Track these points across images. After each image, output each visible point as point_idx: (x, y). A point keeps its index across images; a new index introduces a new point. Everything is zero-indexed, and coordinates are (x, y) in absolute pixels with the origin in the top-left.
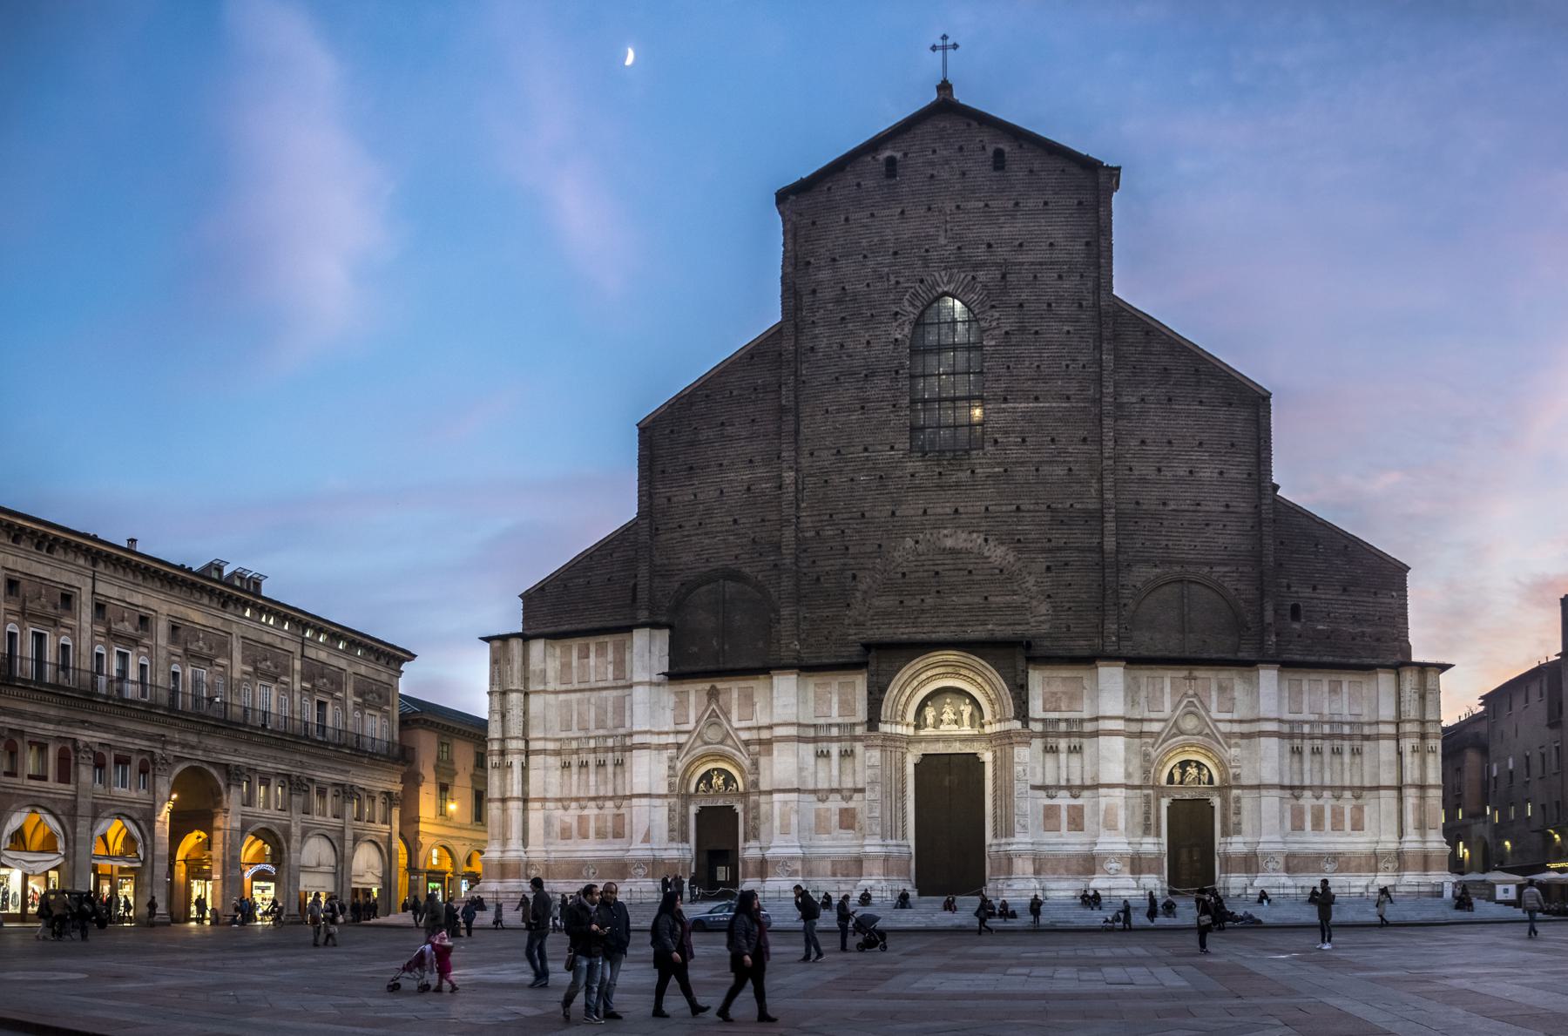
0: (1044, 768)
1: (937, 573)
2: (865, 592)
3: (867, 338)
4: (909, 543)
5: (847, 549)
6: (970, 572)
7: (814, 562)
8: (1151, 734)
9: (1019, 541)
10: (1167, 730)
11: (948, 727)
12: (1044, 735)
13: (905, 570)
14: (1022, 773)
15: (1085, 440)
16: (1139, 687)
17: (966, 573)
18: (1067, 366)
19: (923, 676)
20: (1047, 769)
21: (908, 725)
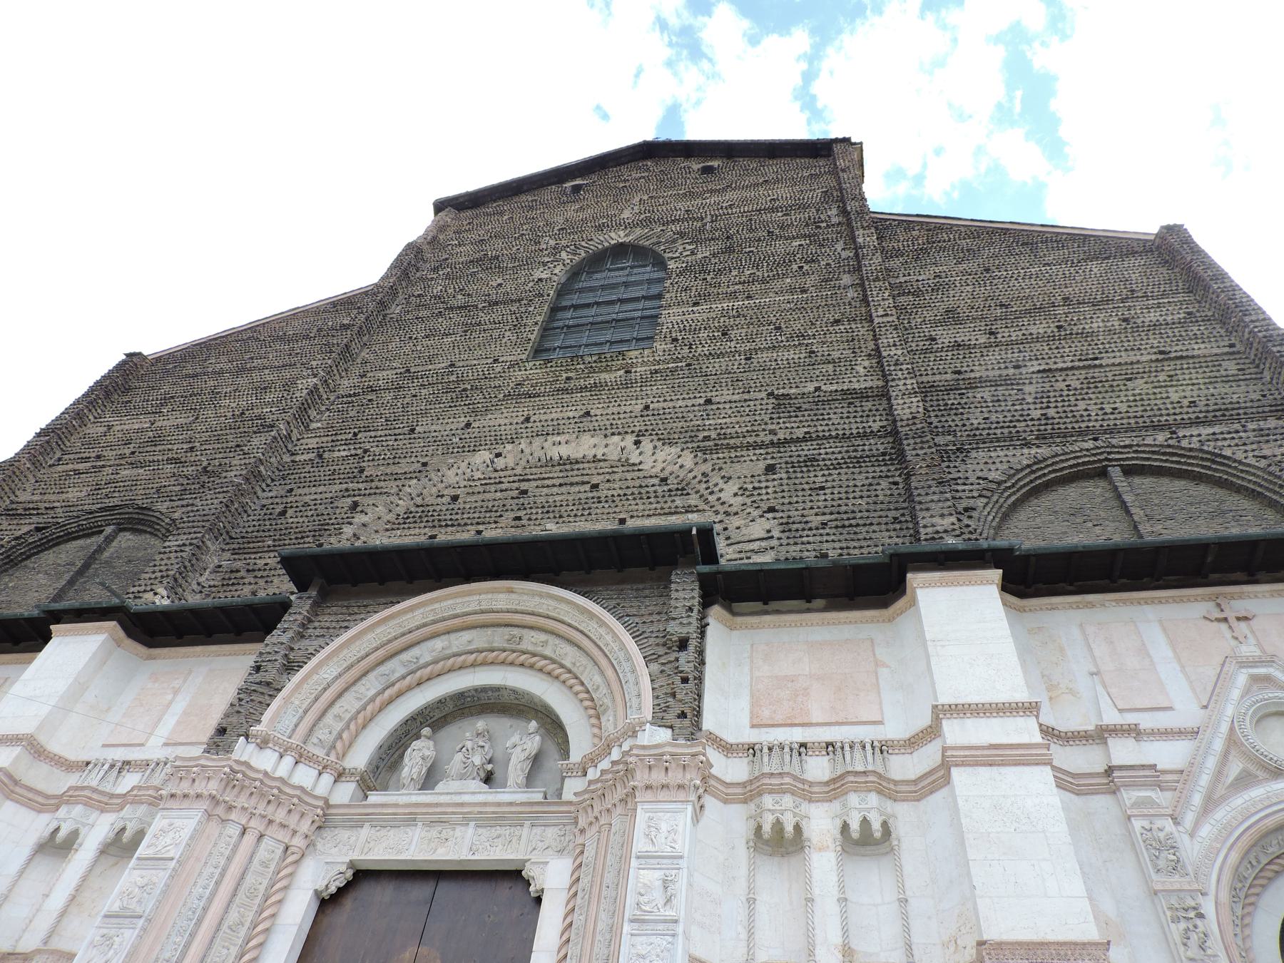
0: (751, 901)
1: (525, 492)
2: (364, 525)
3: (500, 281)
4: (484, 456)
5: (362, 471)
6: (595, 487)
7: (291, 490)
8: (1151, 775)
9: (707, 438)
10: (1211, 763)
11: (454, 785)
12: (749, 792)
13: (459, 492)
14: (658, 896)
15: (837, 322)
16: (1062, 650)
17: (587, 487)
18: (801, 268)
19: (425, 653)
20: (761, 908)
21: (340, 776)
